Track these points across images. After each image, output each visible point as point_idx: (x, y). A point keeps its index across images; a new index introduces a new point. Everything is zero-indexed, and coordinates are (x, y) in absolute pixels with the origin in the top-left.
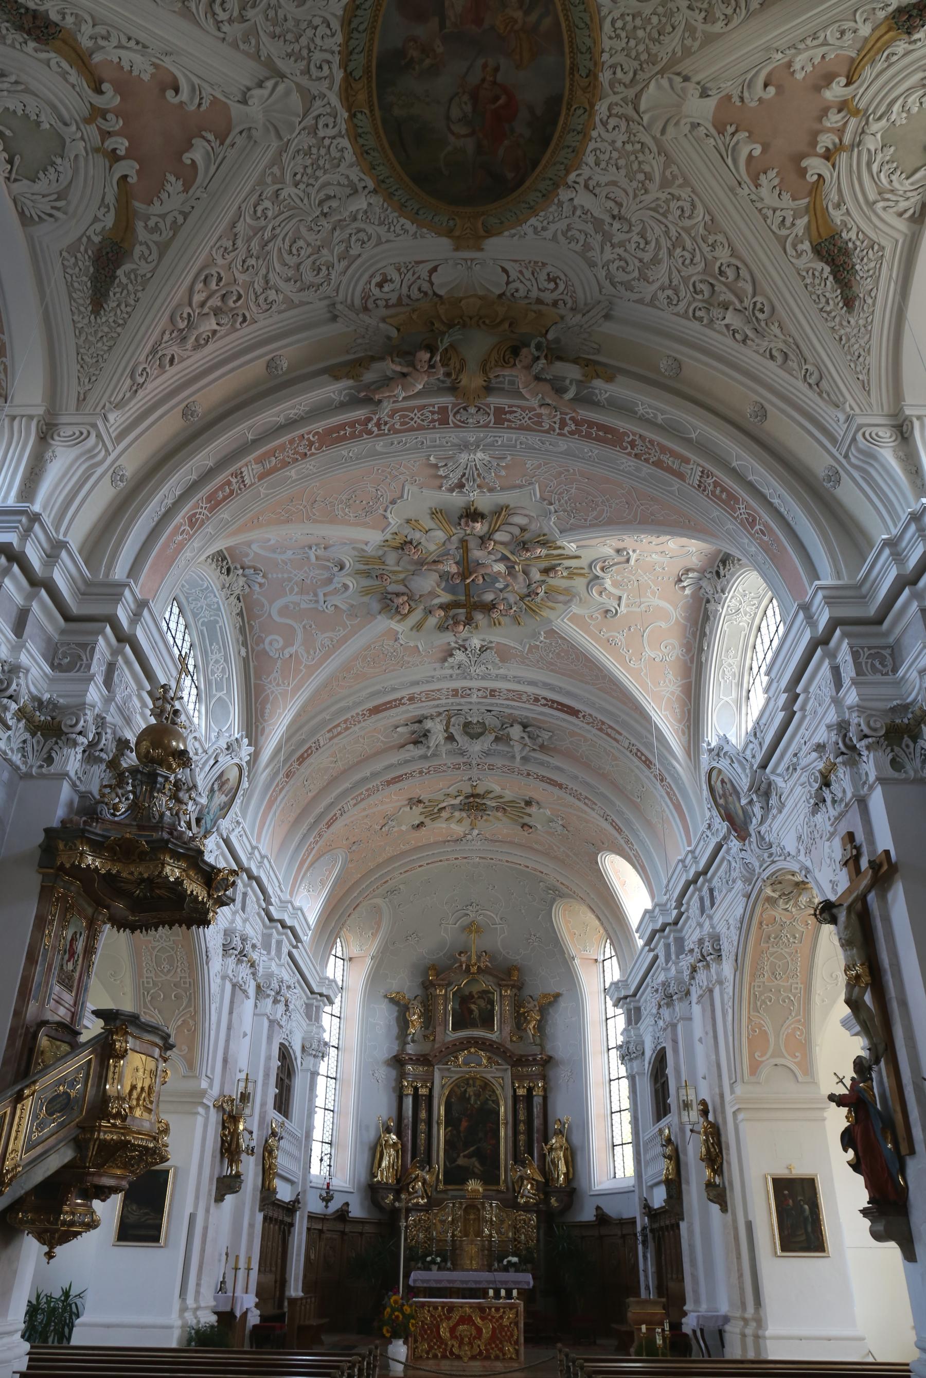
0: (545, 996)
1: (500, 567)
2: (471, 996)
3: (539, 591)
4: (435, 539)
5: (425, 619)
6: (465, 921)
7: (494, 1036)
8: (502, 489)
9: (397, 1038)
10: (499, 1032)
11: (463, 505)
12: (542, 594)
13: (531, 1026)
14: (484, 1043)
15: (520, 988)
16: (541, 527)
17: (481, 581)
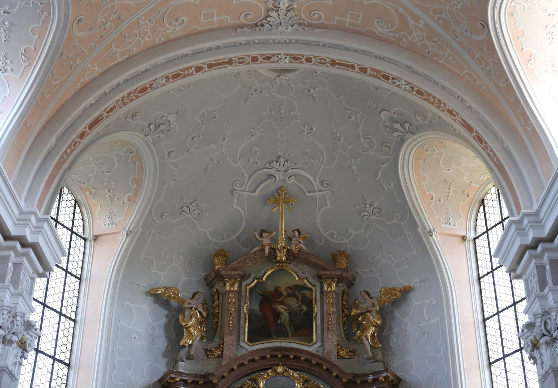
0: (388, 291)
2: (277, 293)
6: (269, 186)
7: (313, 349)
9: (165, 355)
10: (323, 343)
13: (369, 334)
14: (297, 358)
15: (350, 284)
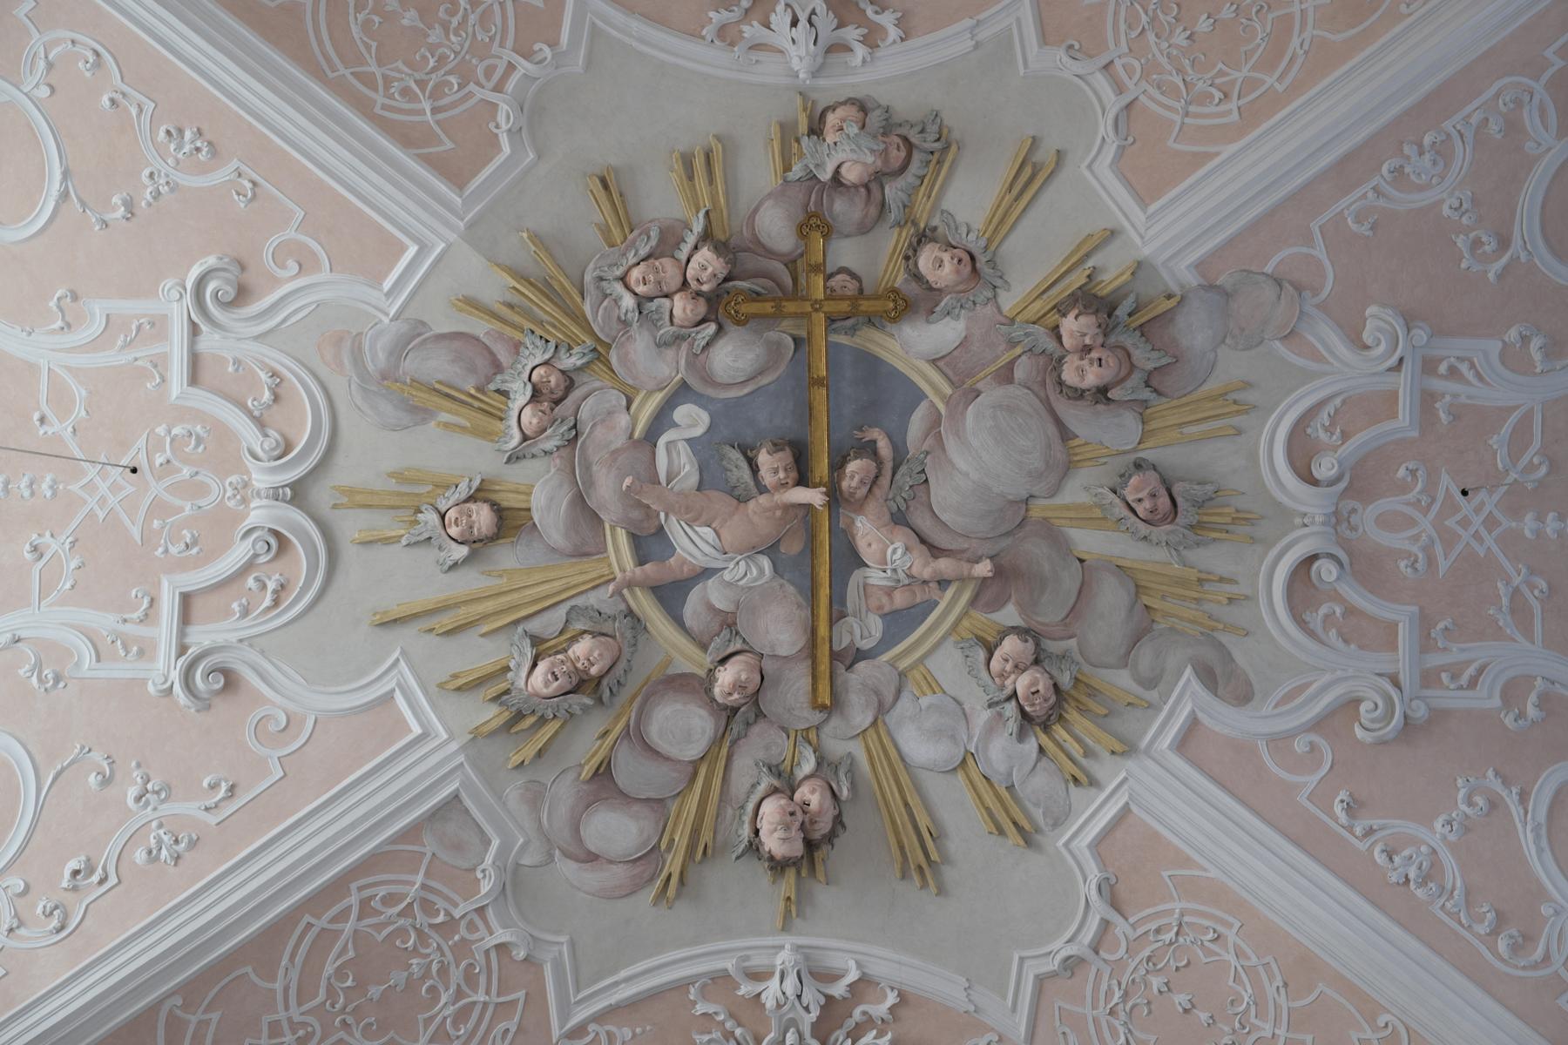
1: (692, 543)
3: (530, 418)
4: (941, 714)
5: (1002, 222)
8: (682, 986)
11: (824, 896)
12: (521, 394)
16: (535, 797)
17: (764, 459)
